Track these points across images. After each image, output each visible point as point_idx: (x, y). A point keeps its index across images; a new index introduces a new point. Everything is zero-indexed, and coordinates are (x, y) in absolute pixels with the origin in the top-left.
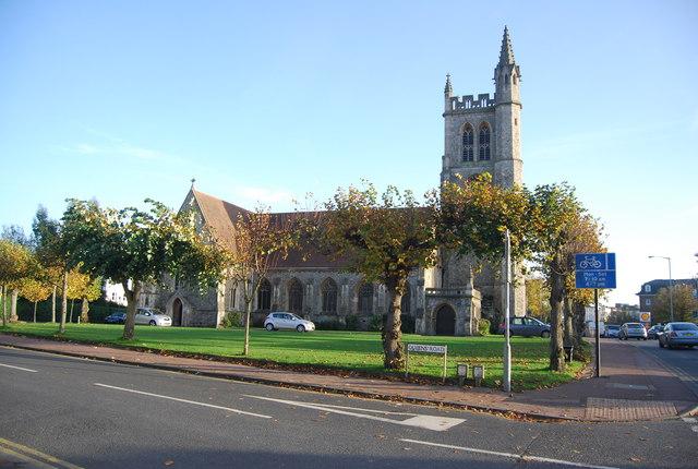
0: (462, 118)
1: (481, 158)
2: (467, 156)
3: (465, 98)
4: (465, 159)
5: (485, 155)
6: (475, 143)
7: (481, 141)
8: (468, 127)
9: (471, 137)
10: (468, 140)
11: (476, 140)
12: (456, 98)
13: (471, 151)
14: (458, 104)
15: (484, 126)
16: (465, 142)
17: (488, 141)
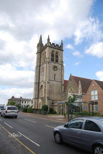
0: (52, 49)
1: (56, 62)
2: (52, 60)
3: (53, 44)
4: (52, 61)
5: (57, 61)
6: (55, 56)
7: (56, 57)
8: (53, 51)
9: (53, 55)
10: (53, 55)
11: (55, 56)
12: (50, 43)
13: (53, 59)
14: (51, 45)
15: (57, 53)
16: (52, 56)
17: (57, 58)
